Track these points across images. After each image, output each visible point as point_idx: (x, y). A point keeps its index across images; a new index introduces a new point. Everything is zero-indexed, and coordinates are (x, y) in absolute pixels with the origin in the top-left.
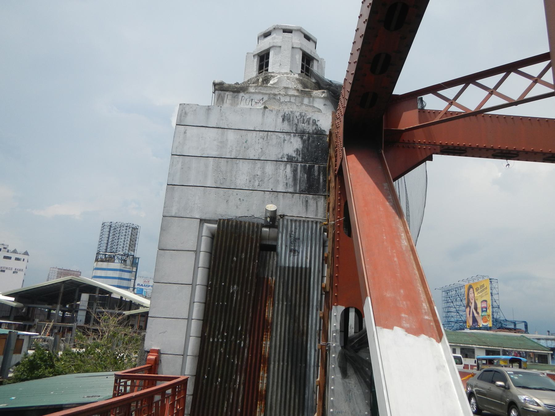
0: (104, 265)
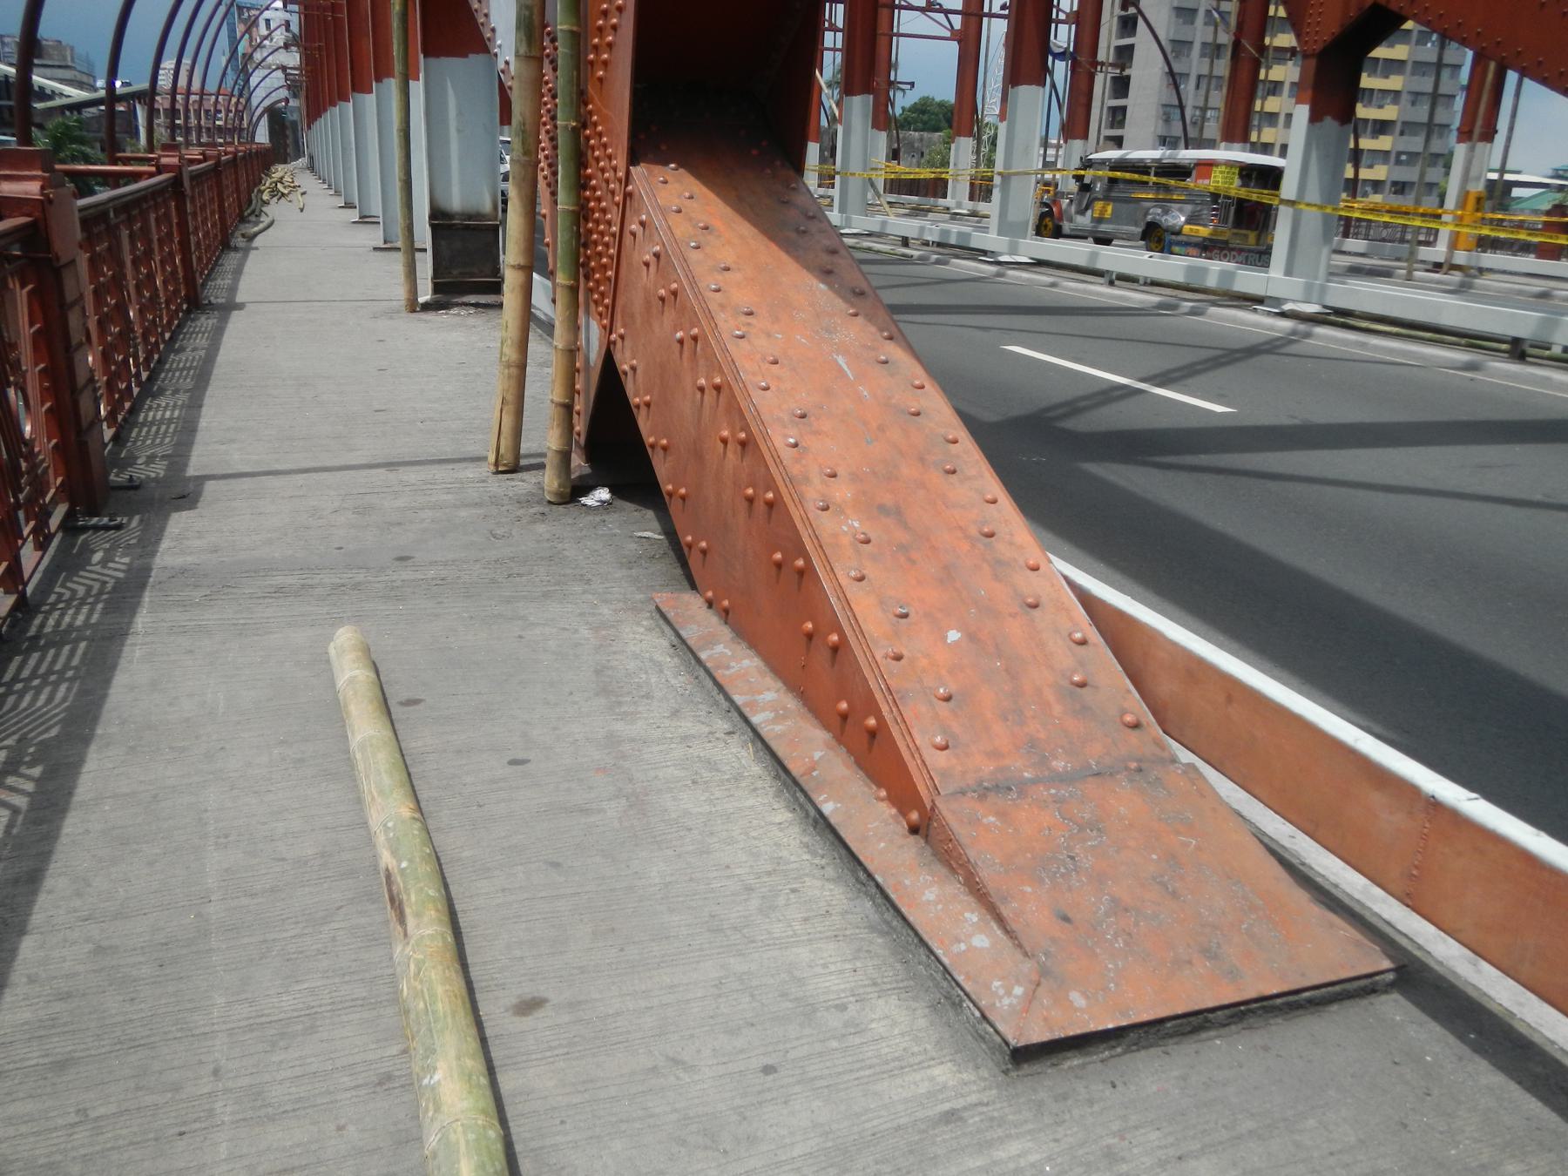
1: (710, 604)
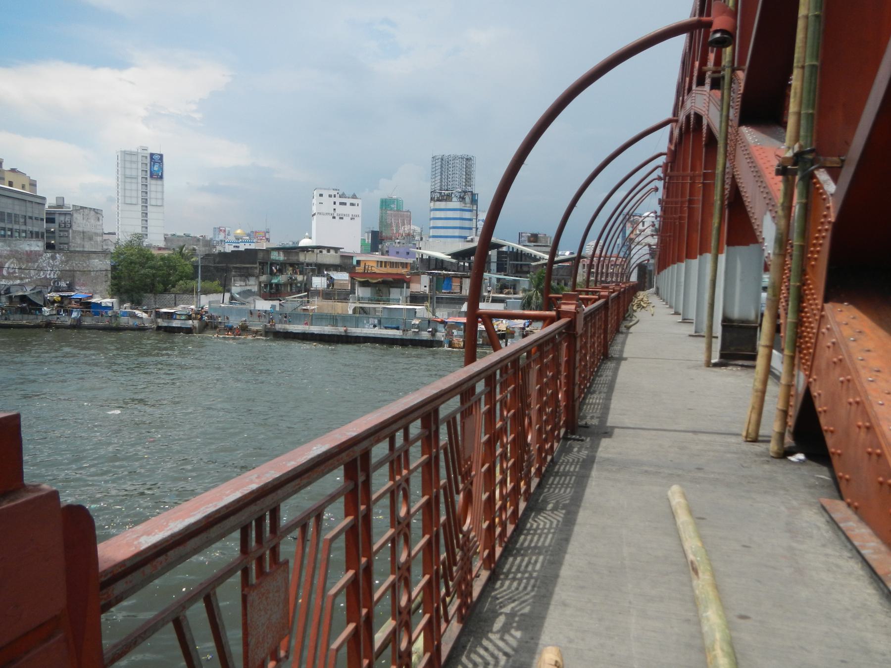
0: (442, 205)
1: (849, 505)
